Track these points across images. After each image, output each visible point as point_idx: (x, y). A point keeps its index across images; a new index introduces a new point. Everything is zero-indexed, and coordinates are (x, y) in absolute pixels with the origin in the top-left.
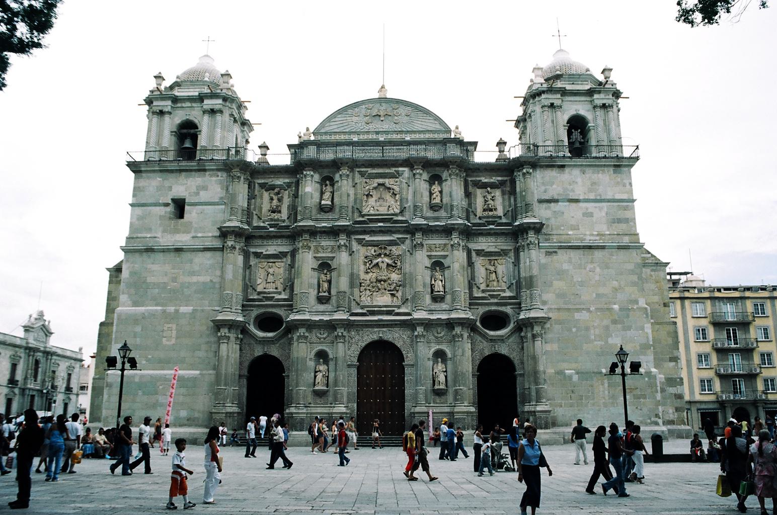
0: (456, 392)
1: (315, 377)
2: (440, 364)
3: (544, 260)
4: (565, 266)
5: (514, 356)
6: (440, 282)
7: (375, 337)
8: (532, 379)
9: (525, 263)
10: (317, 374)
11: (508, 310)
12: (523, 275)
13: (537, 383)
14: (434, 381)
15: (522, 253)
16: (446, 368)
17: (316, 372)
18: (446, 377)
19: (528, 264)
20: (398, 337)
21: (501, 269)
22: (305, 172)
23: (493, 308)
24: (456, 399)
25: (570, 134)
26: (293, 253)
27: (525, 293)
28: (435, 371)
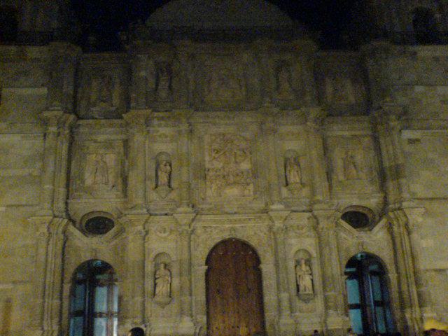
0: (326, 300)
1: (155, 285)
2: (304, 266)
3: (408, 148)
4: (430, 155)
5: (386, 255)
6: (296, 173)
7: (226, 235)
8: (412, 280)
9: (388, 151)
10: (157, 281)
11: (373, 202)
12: (386, 164)
13: (417, 283)
14: (298, 286)
15: (382, 141)
16: (311, 269)
17: (156, 279)
18: (312, 280)
19: (392, 152)
20: (253, 232)
21: (359, 158)
22: (139, 56)
23: (355, 202)
24: (327, 307)
25: (415, 26)
26: (126, 143)
27: (391, 185)
28: (299, 274)
